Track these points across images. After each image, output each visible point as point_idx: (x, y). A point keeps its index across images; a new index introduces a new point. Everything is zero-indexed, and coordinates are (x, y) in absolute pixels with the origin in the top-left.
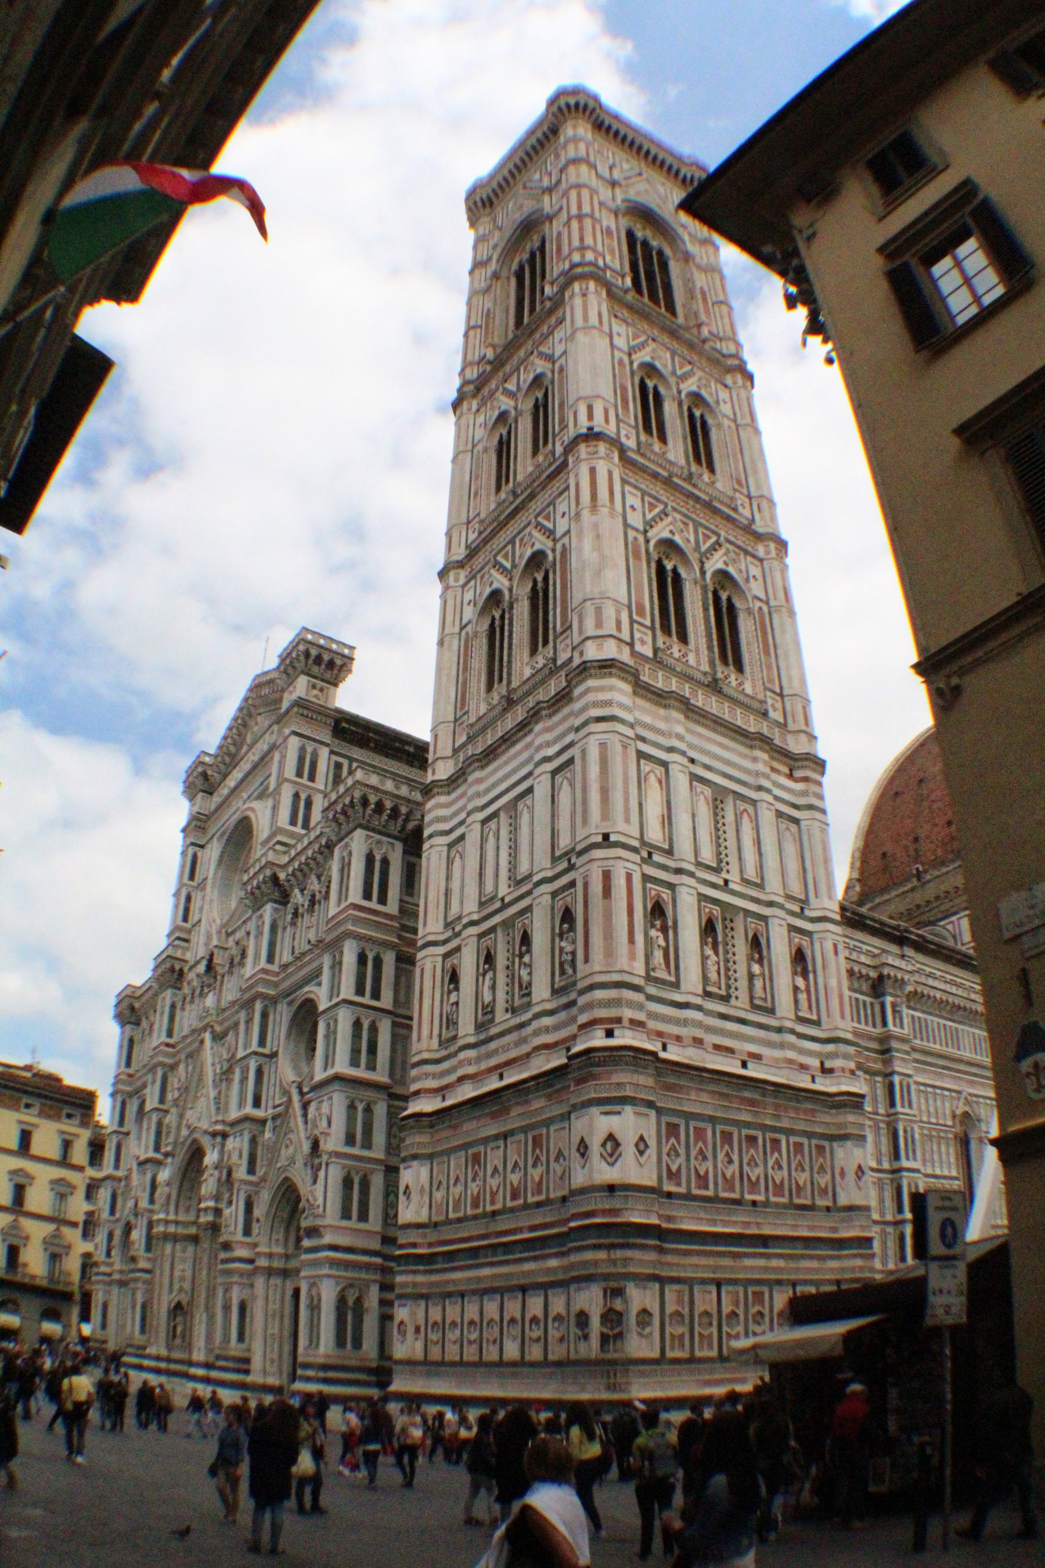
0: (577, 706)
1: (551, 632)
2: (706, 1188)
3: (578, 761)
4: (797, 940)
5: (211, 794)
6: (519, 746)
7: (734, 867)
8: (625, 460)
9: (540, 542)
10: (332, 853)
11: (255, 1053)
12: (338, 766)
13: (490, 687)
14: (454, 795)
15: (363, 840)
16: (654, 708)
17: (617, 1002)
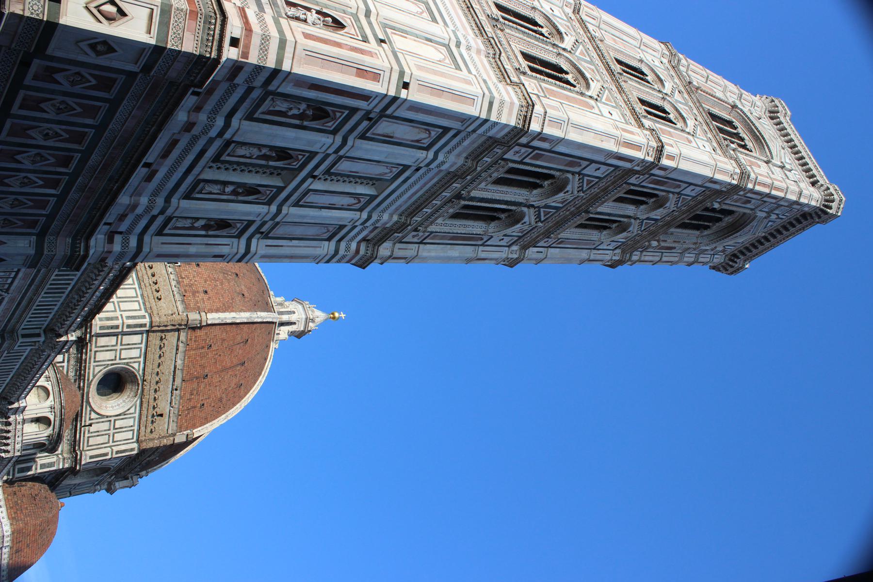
0: (501, 86)
2: (21, 107)
4: (238, 225)
9: (595, 87)
16: (471, 149)
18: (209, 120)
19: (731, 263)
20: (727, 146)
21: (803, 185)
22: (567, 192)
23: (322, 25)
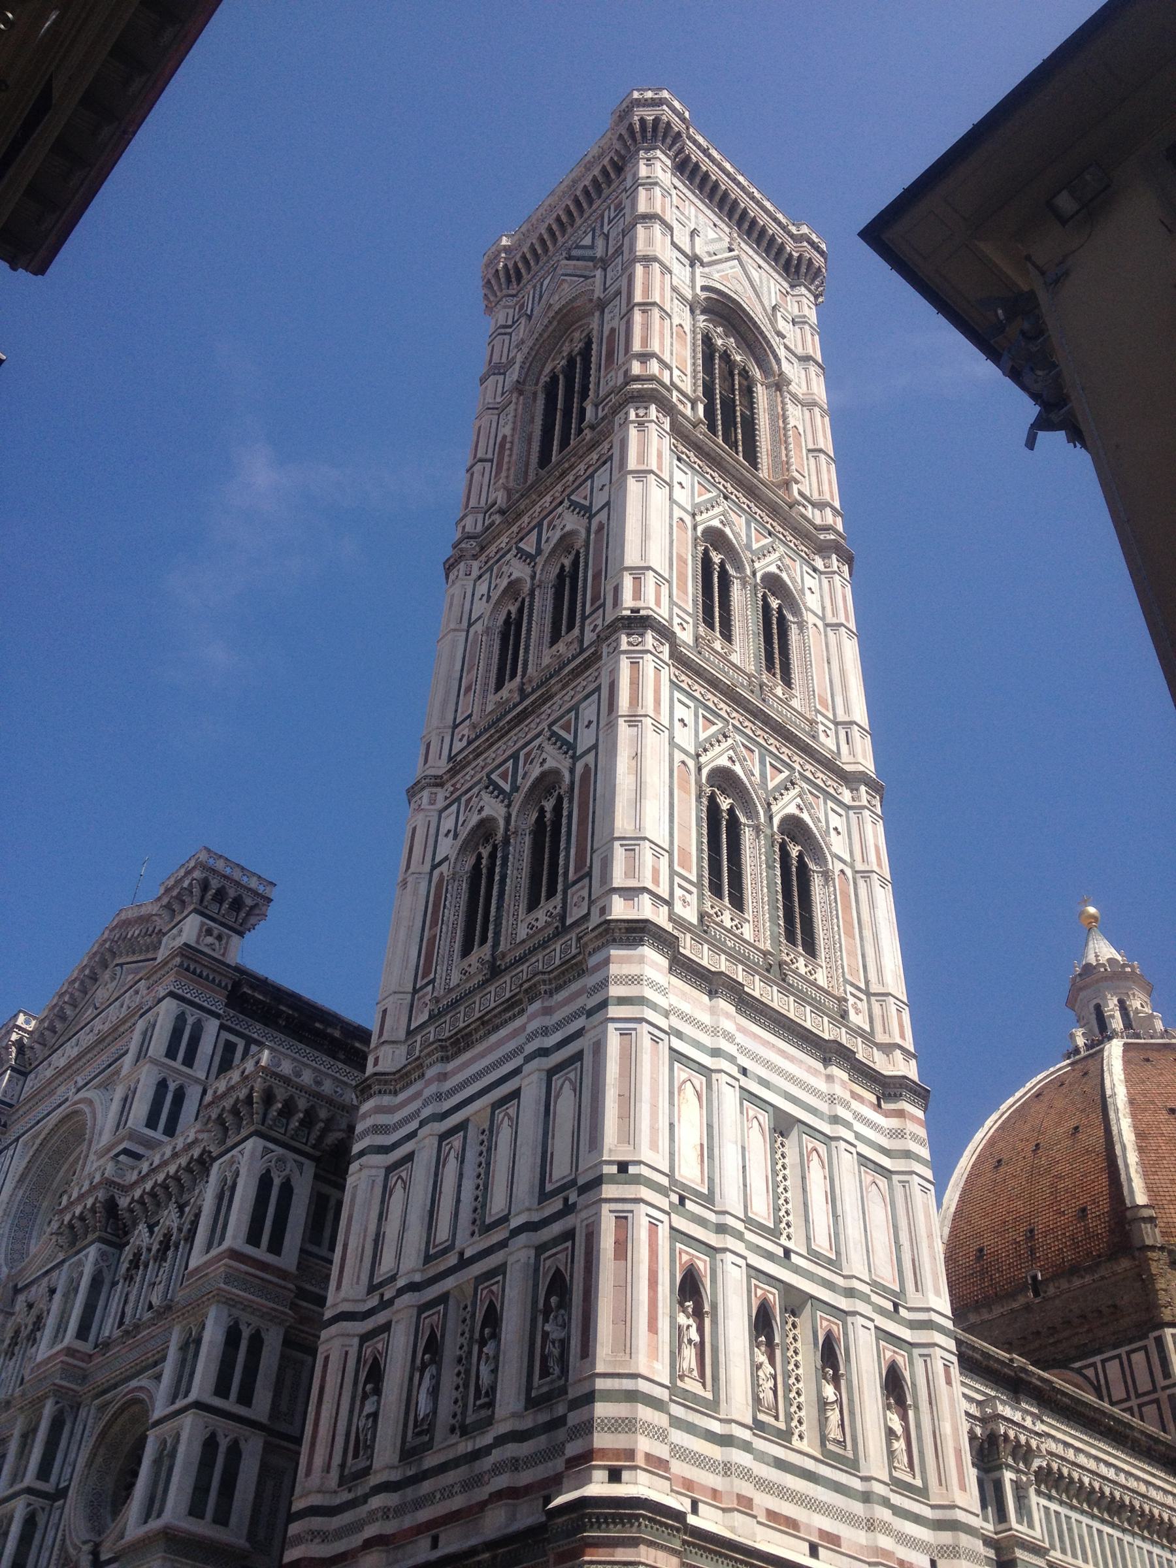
1: (560, 879)
3: (588, 1058)
4: (888, 1354)
5: (25, 1074)
6: (503, 1032)
7: (797, 1230)
8: (678, 658)
9: (554, 759)
10: (206, 1171)
11: (29, 1491)
12: (230, 1048)
13: (466, 951)
14: (402, 1097)
15: (258, 1153)
16: (696, 993)
20: (592, 427)
23: (563, 1312)
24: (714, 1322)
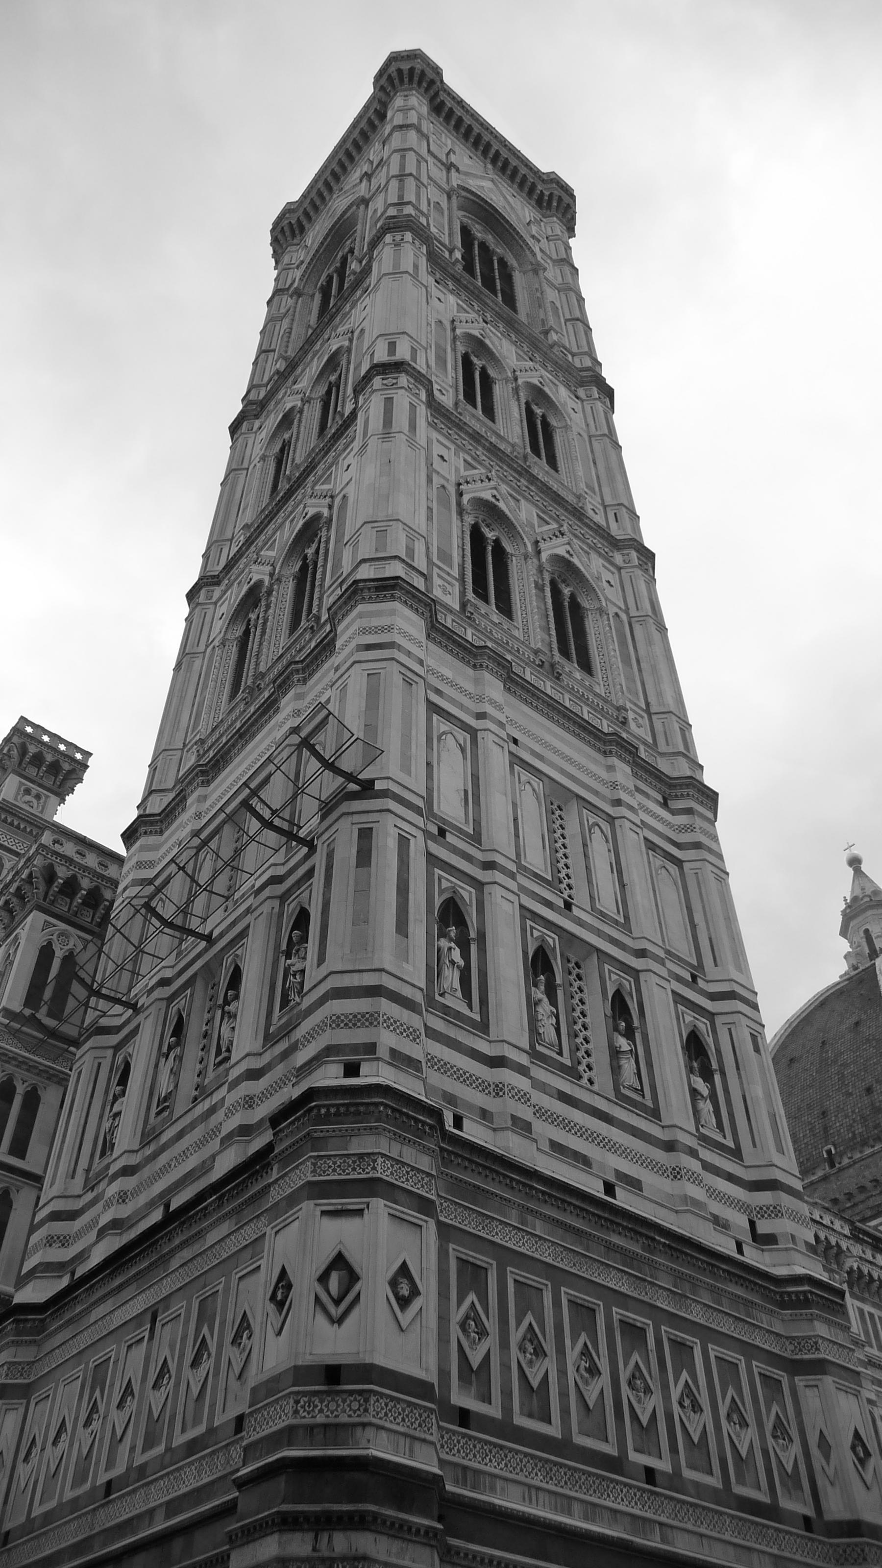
6: (259, 737)
17: (370, 1019)
18: (501, 1094)
19: (555, 204)
21: (388, 129)
22: (494, 496)
24: (482, 950)
